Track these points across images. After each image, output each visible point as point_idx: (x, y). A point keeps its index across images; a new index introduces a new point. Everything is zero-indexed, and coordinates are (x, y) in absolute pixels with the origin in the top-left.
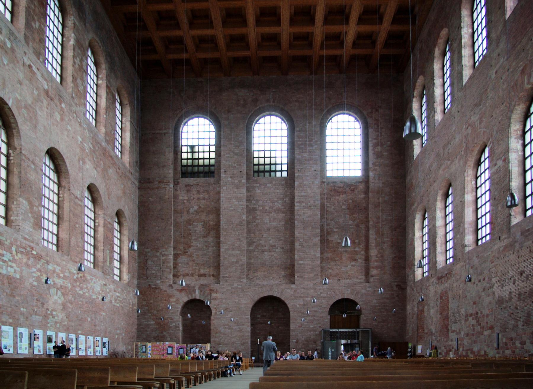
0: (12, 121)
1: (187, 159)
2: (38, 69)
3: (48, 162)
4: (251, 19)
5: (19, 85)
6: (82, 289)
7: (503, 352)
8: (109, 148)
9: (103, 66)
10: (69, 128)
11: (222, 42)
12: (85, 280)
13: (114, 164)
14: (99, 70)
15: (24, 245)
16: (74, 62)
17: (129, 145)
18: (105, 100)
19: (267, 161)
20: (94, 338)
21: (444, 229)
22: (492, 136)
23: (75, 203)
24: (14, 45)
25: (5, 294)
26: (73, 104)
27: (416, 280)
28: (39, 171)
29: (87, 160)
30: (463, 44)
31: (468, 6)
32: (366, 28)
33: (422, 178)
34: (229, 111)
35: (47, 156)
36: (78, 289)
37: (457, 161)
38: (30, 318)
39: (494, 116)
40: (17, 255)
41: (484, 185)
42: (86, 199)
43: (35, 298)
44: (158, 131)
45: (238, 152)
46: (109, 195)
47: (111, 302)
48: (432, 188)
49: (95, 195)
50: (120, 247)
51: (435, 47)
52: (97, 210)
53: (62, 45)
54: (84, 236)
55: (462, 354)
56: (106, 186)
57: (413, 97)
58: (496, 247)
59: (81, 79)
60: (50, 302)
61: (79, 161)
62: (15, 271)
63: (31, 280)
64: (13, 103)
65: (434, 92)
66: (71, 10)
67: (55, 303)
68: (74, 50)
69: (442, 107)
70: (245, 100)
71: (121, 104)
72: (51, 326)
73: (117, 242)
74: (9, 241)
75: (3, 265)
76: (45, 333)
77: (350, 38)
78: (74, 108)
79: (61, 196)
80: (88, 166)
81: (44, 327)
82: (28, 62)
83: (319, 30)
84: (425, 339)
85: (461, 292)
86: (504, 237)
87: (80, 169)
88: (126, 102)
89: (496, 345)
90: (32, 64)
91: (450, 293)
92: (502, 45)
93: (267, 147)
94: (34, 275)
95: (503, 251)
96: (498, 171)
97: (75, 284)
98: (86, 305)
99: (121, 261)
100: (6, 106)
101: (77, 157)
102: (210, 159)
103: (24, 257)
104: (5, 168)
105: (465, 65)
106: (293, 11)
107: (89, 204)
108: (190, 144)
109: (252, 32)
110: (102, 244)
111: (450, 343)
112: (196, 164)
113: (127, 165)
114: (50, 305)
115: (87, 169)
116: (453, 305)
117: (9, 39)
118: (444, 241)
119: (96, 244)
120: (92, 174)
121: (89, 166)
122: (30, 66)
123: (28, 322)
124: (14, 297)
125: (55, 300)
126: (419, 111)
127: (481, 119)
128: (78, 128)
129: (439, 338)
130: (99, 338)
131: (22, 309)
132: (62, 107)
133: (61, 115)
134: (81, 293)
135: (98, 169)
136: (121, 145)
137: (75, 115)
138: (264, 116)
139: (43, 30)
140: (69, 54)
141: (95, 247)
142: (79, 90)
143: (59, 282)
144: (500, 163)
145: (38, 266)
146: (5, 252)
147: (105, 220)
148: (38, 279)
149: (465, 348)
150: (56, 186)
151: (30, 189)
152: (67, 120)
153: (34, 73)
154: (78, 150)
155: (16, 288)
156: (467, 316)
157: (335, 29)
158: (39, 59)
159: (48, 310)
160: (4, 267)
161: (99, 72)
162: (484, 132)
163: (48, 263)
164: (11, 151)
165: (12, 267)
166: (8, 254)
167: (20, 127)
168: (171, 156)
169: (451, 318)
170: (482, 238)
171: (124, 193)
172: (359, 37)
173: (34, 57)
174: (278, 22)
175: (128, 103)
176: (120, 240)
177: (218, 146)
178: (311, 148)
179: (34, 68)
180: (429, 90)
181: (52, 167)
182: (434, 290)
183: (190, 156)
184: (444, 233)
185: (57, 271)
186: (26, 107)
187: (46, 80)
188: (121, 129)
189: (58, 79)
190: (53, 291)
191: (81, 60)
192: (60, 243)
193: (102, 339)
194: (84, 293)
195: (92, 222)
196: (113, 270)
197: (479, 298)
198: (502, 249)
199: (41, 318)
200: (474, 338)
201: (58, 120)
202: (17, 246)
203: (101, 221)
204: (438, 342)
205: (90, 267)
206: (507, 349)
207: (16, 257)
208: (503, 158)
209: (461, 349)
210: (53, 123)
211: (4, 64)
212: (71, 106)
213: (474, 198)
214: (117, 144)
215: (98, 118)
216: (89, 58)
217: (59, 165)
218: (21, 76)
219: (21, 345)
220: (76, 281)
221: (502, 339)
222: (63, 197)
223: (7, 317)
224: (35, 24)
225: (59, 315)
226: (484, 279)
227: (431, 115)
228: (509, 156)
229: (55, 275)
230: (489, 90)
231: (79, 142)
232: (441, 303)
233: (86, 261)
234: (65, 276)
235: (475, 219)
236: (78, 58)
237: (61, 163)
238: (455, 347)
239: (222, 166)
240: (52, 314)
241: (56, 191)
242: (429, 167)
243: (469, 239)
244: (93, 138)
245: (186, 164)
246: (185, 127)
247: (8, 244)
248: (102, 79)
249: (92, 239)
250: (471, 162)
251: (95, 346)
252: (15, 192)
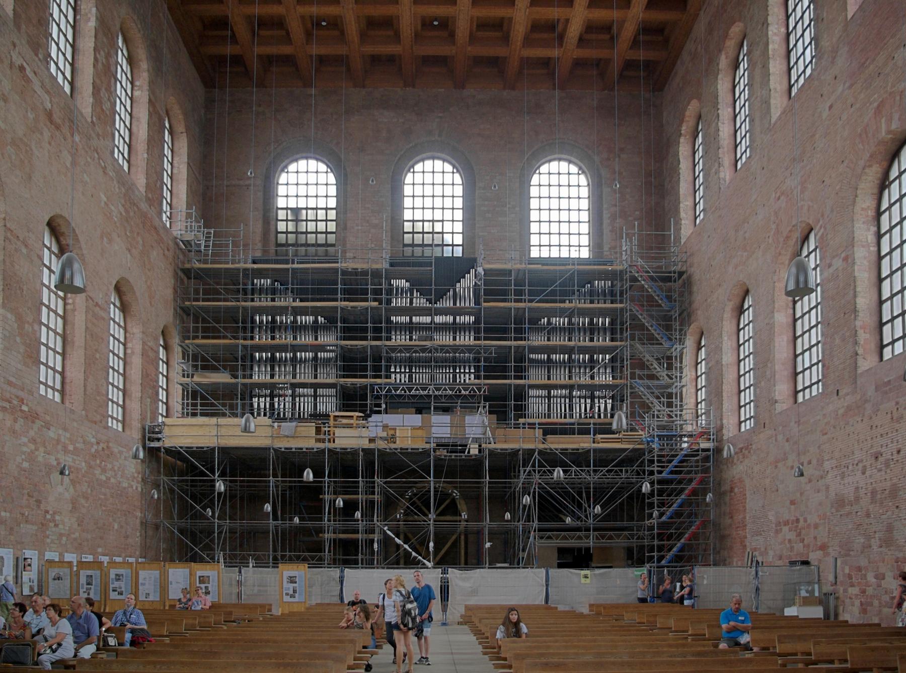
2: (35, 73)
9: (144, 65)
14: (135, 71)
16: (96, 59)
26: (94, 135)
36: (98, 472)
43: (26, 491)
49: (128, 298)
52: (129, 325)
59: (106, 89)
71: (171, 133)
72: (52, 542)
76: (41, 555)
81: (40, 545)
82: (18, 61)
90: (25, 64)
94: (25, 449)
97: (92, 463)
107: (115, 313)
119: (128, 386)
122: (22, 68)
125: (60, 494)
134: (104, 478)
135: (134, 250)
137: (96, 155)
140: (88, 44)
142: (103, 110)
145: (32, 433)
147: (144, 343)
151: (18, 292)
153: (28, 81)
158: (37, 55)
159: (47, 512)
163: (48, 426)
179: (28, 70)
185: (63, 439)
187: (48, 92)
192: (67, 387)
199: (35, 527)
203: (136, 346)
212: (89, 138)
215: (133, 158)
216: (120, 52)
220: (94, 457)
222: (73, 303)
225: (66, 520)
229: (60, 447)
234: (75, 448)
236: (102, 53)
240: (54, 521)
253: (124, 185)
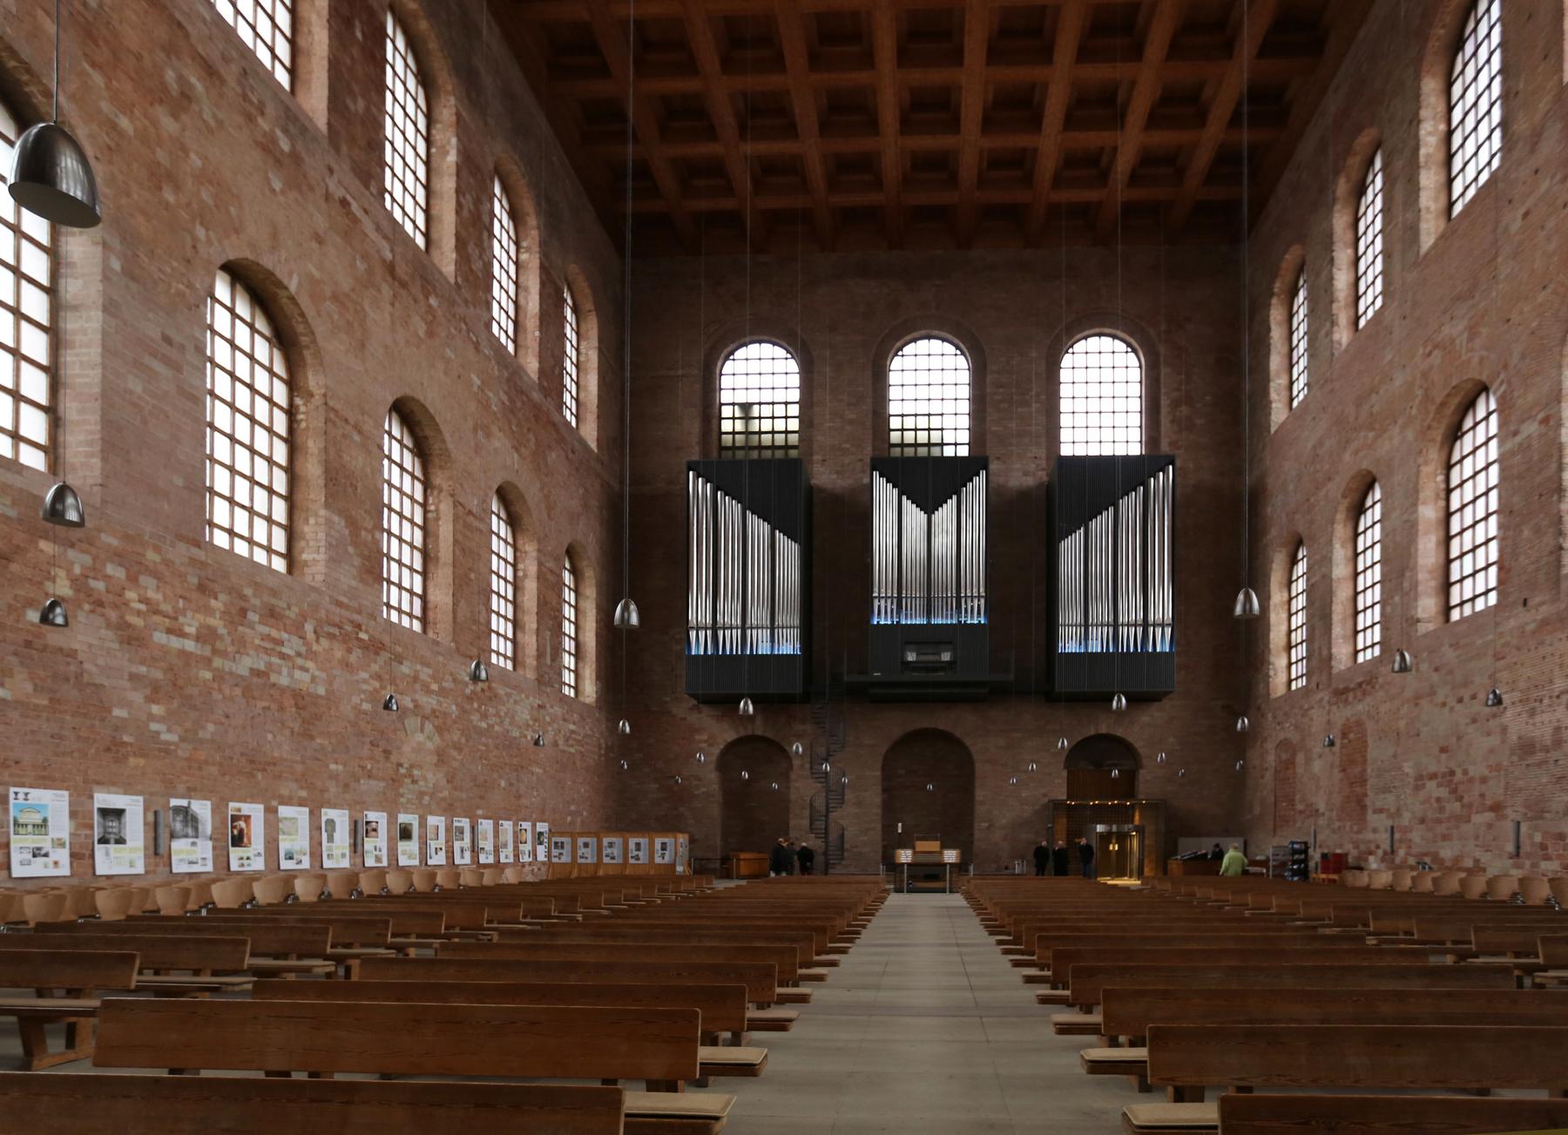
0: (300, 328)
1: (734, 433)
2: (366, 211)
3: (396, 432)
4: (889, 117)
5: (314, 245)
6: (484, 716)
7: (1534, 865)
8: (549, 405)
9: (532, 221)
10: (449, 353)
11: (817, 170)
12: (493, 697)
13: (561, 440)
14: (521, 229)
15: (337, 619)
16: (459, 204)
17: (595, 401)
18: (537, 297)
19: (922, 437)
20: (515, 825)
21: (1350, 584)
22: (1505, 367)
23: (468, 526)
24: (299, 147)
25: (287, 732)
26: (459, 300)
27: (1273, 696)
28: (376, 450)
29: (494, 429)
30: (1422, 159)
31: (1440, 69)
32: (1163, 139)
33: (1294, 473)
35: (394, 415)
36: (475, 718)
37: (1397, 430)
38: (353, 785)
39: (1515, 318)
40: (317, 641)
41: (1470, 483)
42: (494, 518)
43: (367, 740)
46: (550, 508)
47: (556, 744)
48: (1322, 494)
49: (517, 508)
50: (576, 624)
51: (1337, 173)
52: (520, 543)
53: (427, 163)
54: (489, 600)
55: (1404, 861)
56: (542, 489)
57: (1272, 294)
58: (1512, 623)
60: (406, 749)
61: (475, 430)
62: (313, 679)
63: (355, 700)
64: (300, 284)
65: (1331, 279)
66: (445, 79)
67: (419, 749)
68: (458, 175)
69: (1352, 312)
71: (575, 310)
72: (409, 801)
73: (569, 612)
74: (295, 609)
75: (280, 666)
76: (392, 819)
77: (1123, 164)
78: (461, 310)
79: (432, 508)
80: (497, 444)
81: (391, 806)
82: (339, 193)
83: (1050, 142)
84: (1298, 825)
85: (1402, 724)
86: (1537, 600)
87: (478, 449)
88: (588, 305)
89: (1510, 848)
90: (349, 198)
91: (1370, 726)
92: (1550, 145)
93: (923, 408)
94: (365, 687)
95: (1534, 632)
96: (1524, 448)
97: (468, 707)
98: (495, 752)
99: (578, 655)
100: (282, 293)
101: (470, 423)
102: (786, 432)
103: (336, 645)
104: (285, 440)
105: (1428, 209)
106: (990, 97)
107: (499, 526)
108: (741, 397)
109: (892, 147)
110: (534, 618)
111: (1370, 836)
112: (756, 443)
113: (593, 445)
114: (406, 754)
115: (495, 450)
116: (1378, 752)
117: (285, 131)
118: (1350, 611)
119: (520, 616)
120: (509, 462)
121: (500, 442)
122: (344, 203)
123: (347, 796)
124: (312, 738)
125: (419, 743)
126: (1285, 326)
127: (1473, 332)
128: (471, 353)
129: (1337, 824)
130: (526, 825)
131: (333, 767)
132: (430, 306)
133: (429, 324)
134: (484, 725)
135: (523, 450)
136: (577, 400)
138: (915, 340)
139: (375, 118)
140: (447, 185)
141: (516, 623)
143: (429, 702)
144: (1531, 428)
145: (375, 667)
146: (285, 636)
147: (540, 564)
148: (373, 696)
149: (1415, 850)
150: (419, 487)
151: (350, 490)
152: (443, 335)
153: (355, 220)
154: (472, 406)
155: (318, 717)
156: (1419, 777)
157: (1090, 139)
158: (367, 187)
159: (401, 765)
160: (285, 671)
161: (521, 235)
162: (1482, 359)
163: (399, 659)
164: (298, 401)
165: (307, 670)
166: (295, 639)
167: (321, 343)
168: (693, 427)
169: (1371, 782)
170: (1462, 603)
171: (585, 506)
172: (1147, 160)
173: (355, 184)
174: (954, 125)
176: (576, 608)
177: (806, 403)
178: (1025, 409)
179: (354, 206)
180: (1318, 275)
181: (407, 441)
182: (1322, 718)
183: (739, 426)
184: (1350, 592)
185: (423, 676)
186: (335, 298)
187: (386, 237)
188: (577, 366)
189: (420, 241)
190: (412, 722)
191: (477, 202)
192: (431, 615)
193: (534, 826)
194: (491, 726)
195: (510, 569)
196: (560, 675)
197: (1459, 738)
198: (1532, 626)
199: (382, 784)
200: (1441, 829)
201: (421, 333)
202: (319, 621)
203: (530, 567)
204: (1334, 831)
205: (505, 669)
206: (1547, 858)
207: (315, 647)
208: (1541, 416)
209: (1401, 852)
210: (407, 342)
211: (273, 191)
212: (453, 303)
213: (1441, 514)
214: (567, 398)
215: (520, 338)
217: (426, 437)
218: (321, 223)
219: (329, 849)
220: (470, 699)
221: (1531, 837)
222: (437, 510)
223: (294, 786)
224: (355, 102)
225: (430, 776)
226: (1474, 697)
227: (1323, 332)
228: (1559, 411)
229: (418, 686)
230: (1500, 260)
231: (475, 389)
232: (1343, 746)
233: (494, 656)
234: (442, 689)
235: (1442, 560)
237: (429, 432)
238: (1386, 846)
239: (815, 447)
240: (411, 776)
241: (419, 496)
242: (1314, 447)
243: (1427, 605)
244: (508, 380)
245: (730, 444)
246: (728, 364)
247: (293, 616)
248: (528, 250)
249: (510, 607)
250: (1438, 434)
251: (518, 841)
252: (312, 496)
253: (506, 367)
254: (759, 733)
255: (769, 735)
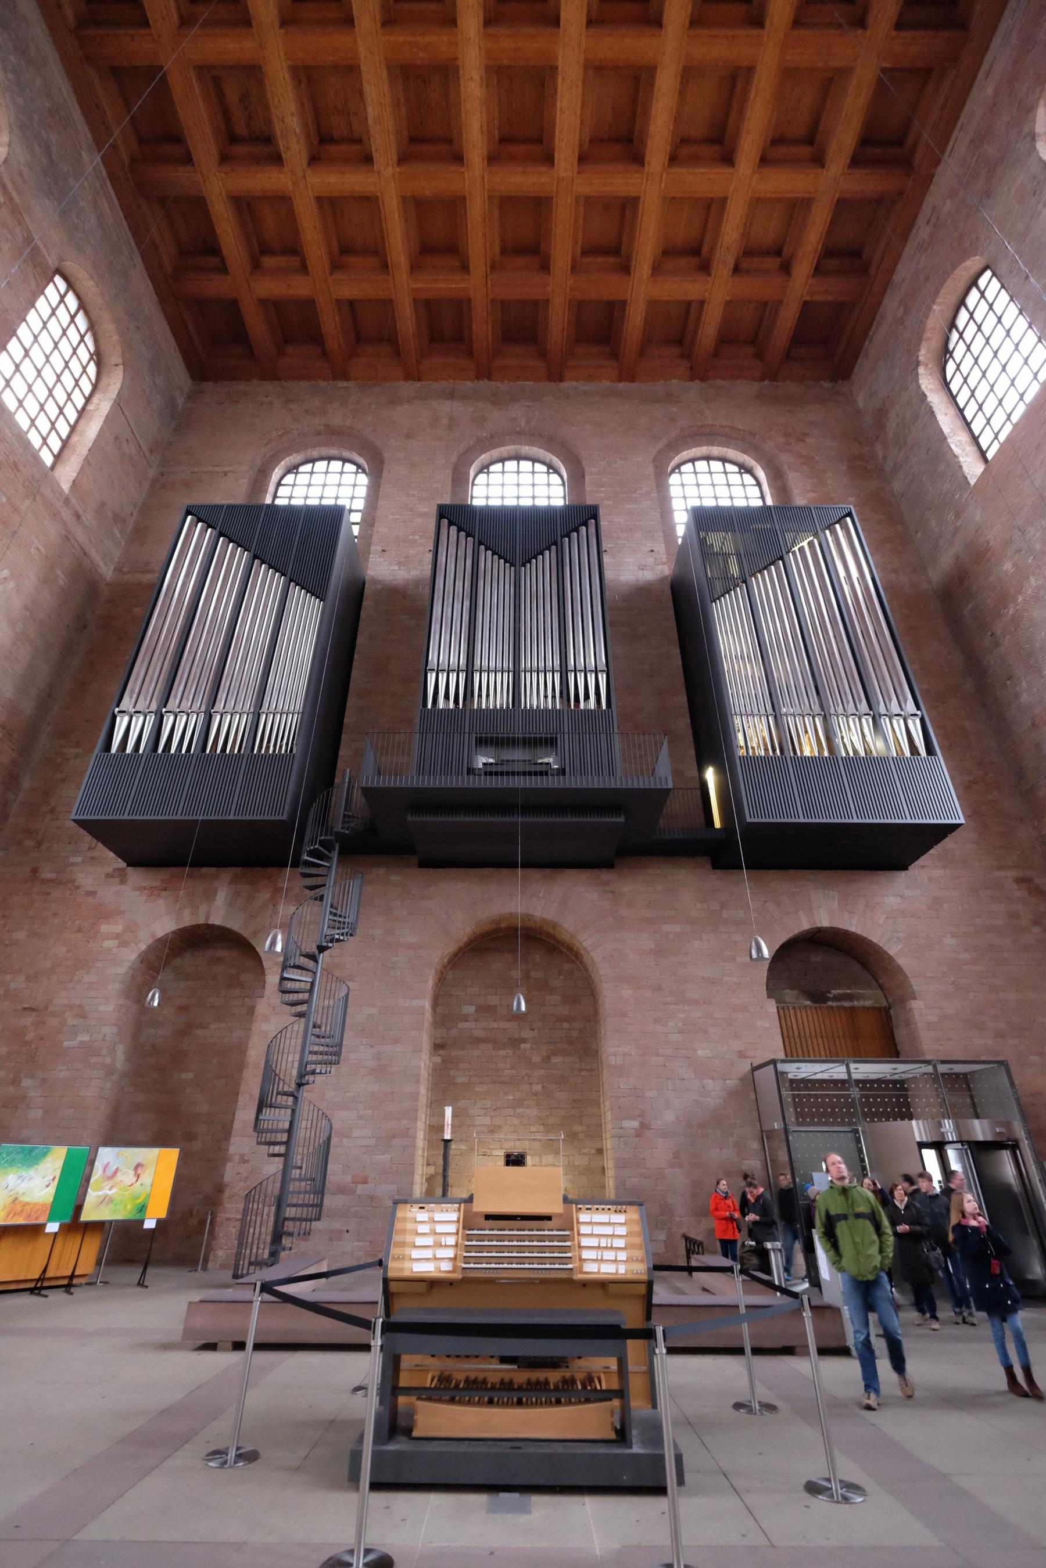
34: (408, 436)
44: (211, 469)
45: (426, 510)
70: (451, 419)
175: (120, 361)
254: (216, 920)
255: (235, 924)
